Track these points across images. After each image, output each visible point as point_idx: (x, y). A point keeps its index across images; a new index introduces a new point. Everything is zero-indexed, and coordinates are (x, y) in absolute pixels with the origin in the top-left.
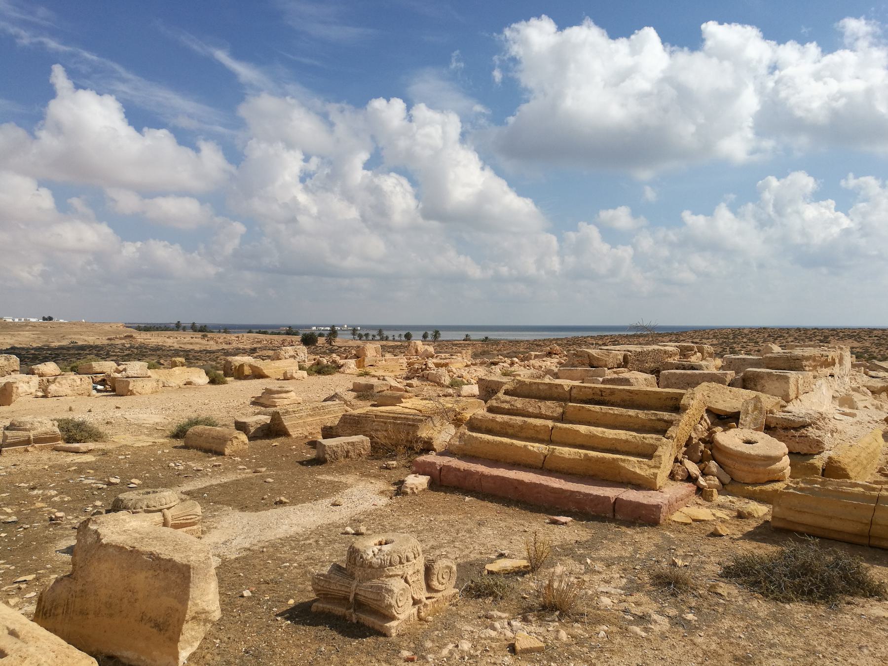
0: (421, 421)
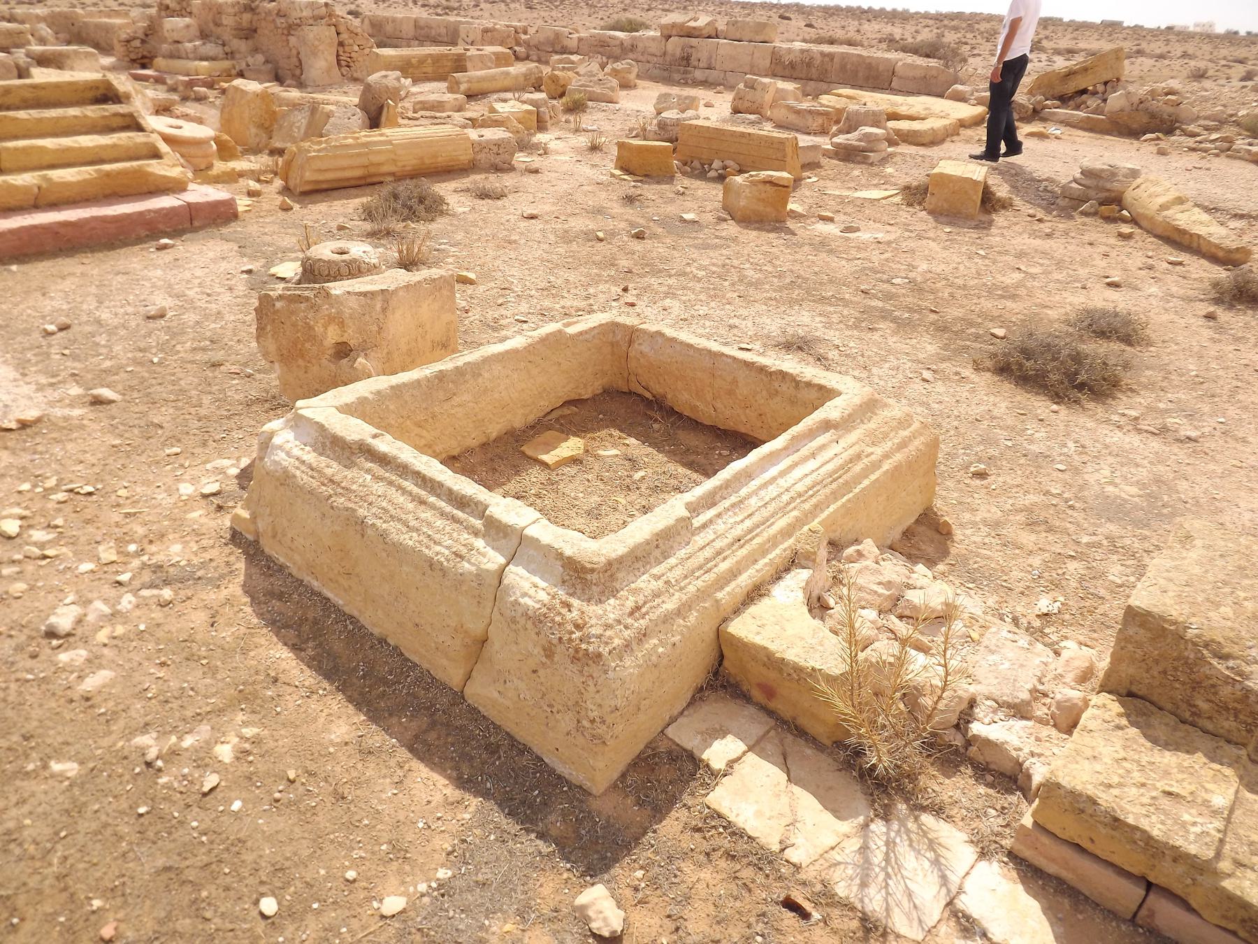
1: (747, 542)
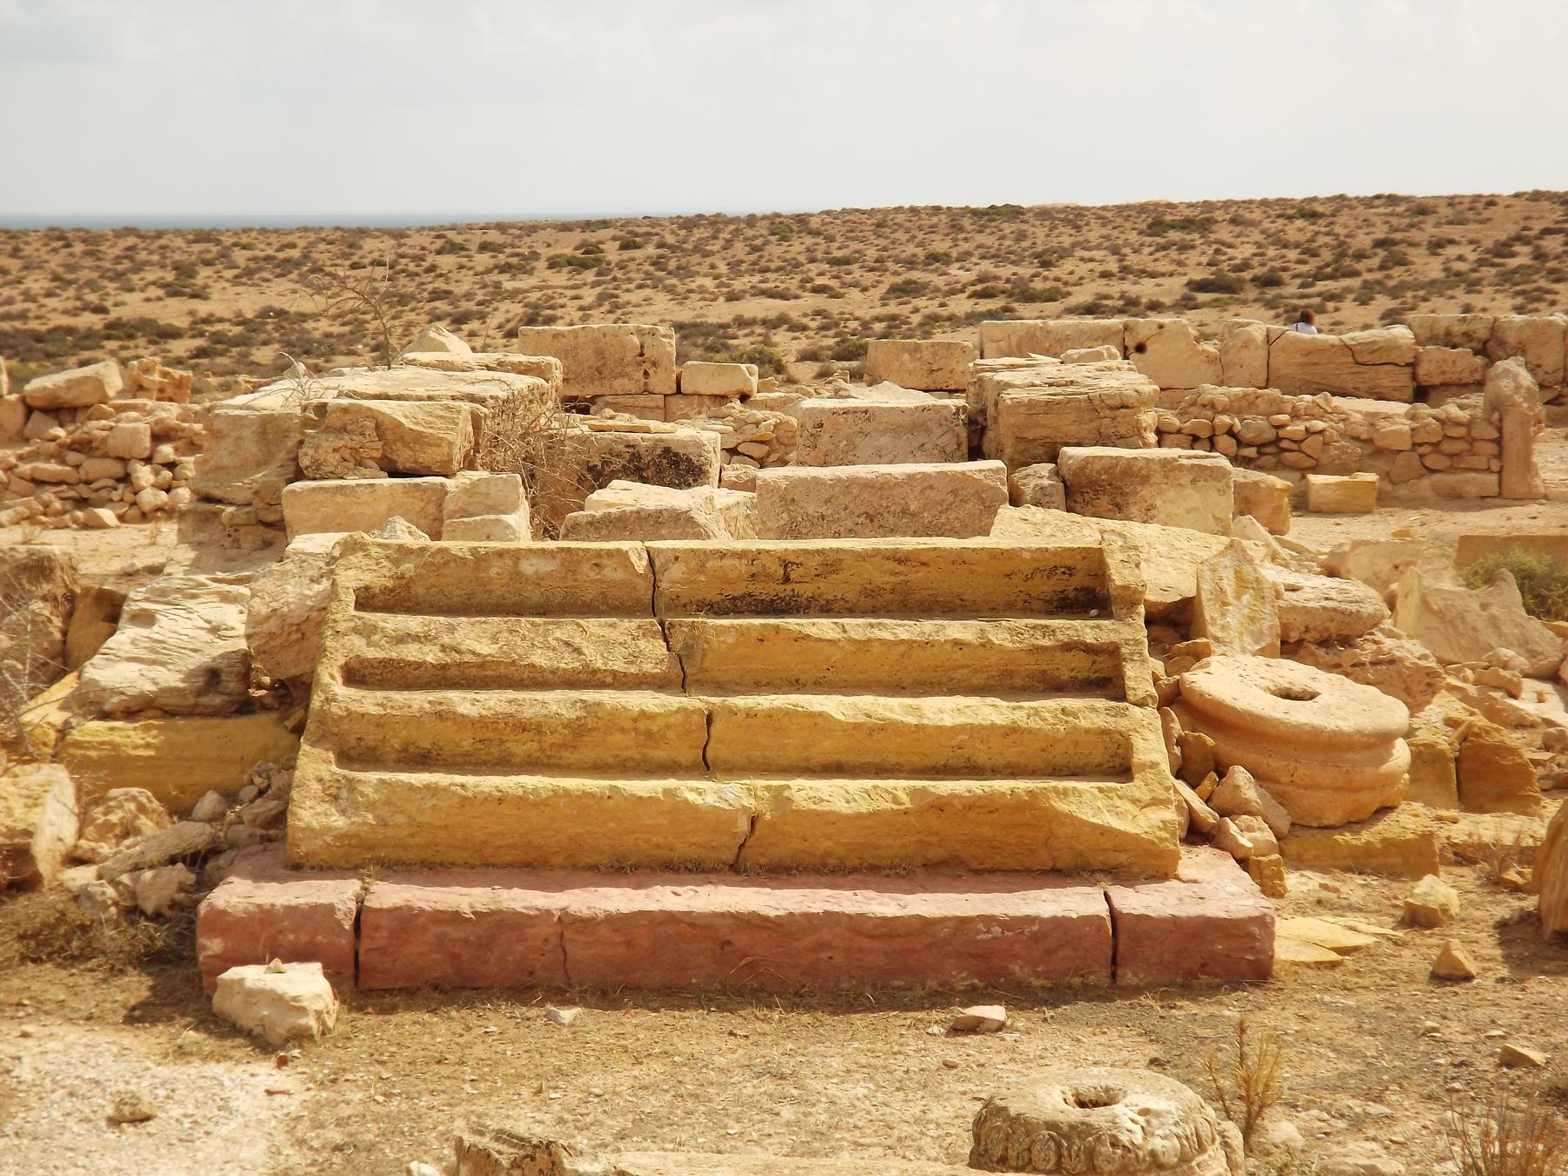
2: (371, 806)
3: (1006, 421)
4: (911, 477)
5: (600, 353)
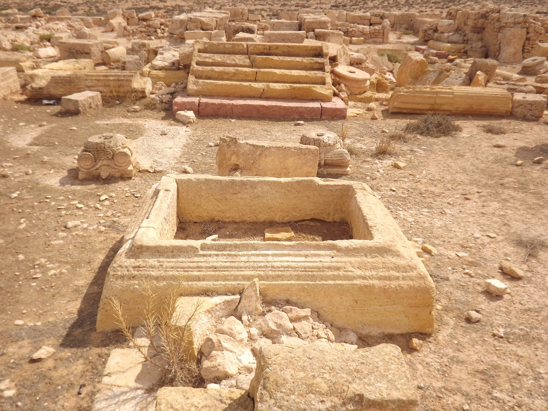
0: (132, 76)
1: (220, 271)
2: (201, 85)
3: (305, 25)
4: (290, 34)
5: (235, 12)
